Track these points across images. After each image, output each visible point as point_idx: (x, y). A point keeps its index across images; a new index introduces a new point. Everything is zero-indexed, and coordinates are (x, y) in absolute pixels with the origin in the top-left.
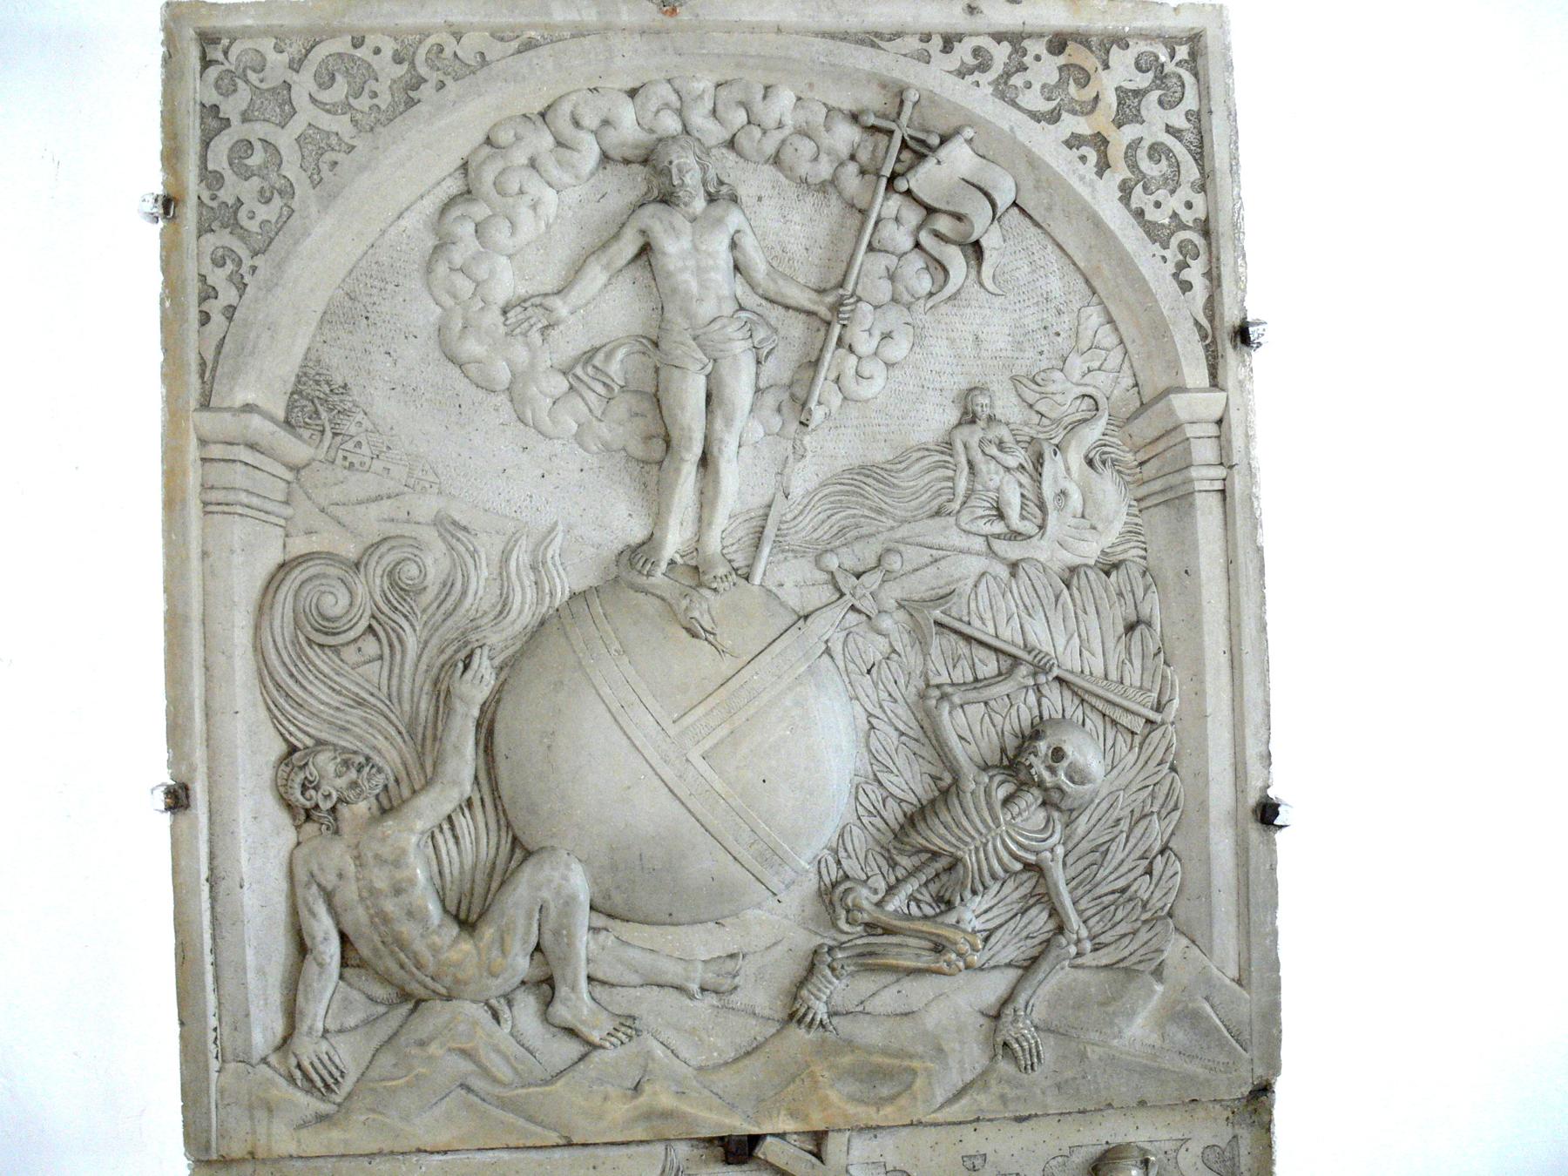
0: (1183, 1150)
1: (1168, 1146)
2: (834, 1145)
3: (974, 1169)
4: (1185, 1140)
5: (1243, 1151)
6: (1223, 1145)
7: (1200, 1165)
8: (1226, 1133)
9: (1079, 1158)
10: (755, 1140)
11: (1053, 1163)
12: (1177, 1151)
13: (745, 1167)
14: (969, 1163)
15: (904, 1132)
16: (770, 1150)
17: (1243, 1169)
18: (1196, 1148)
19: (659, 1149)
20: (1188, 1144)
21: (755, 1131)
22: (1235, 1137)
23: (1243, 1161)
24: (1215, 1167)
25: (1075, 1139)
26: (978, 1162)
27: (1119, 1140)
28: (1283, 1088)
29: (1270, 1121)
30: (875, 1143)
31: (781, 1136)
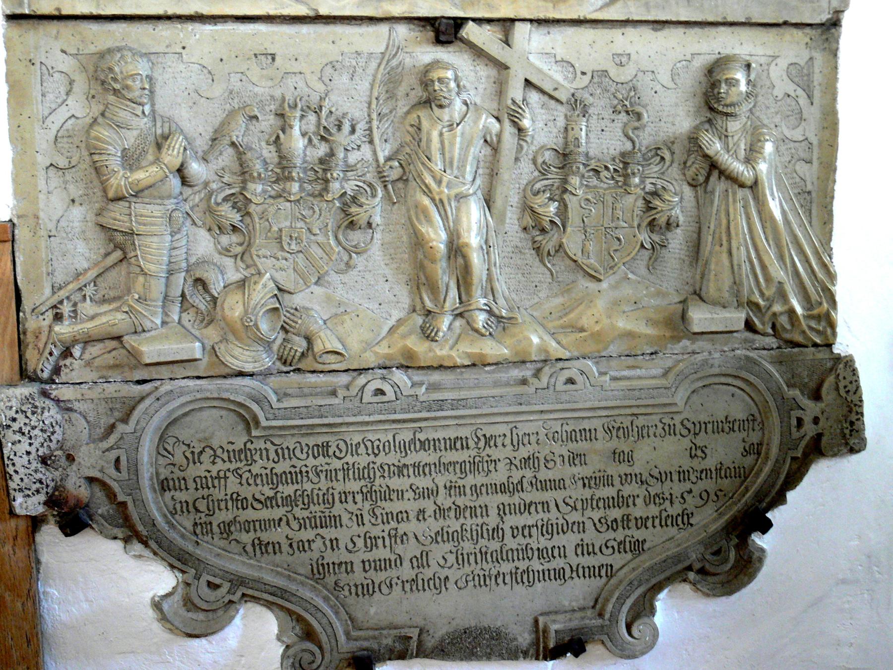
0: (773, 64)
1: (763, 60)
2: (521, 31)
3: (621, 65)
4: (775, 57)
5: (817, 70)
6: (802, 63)
7: (785, 77)
8: (806, 55)
9: (699, 63)
10: (459, 23)
11: (678, 65)
12: (769, 65)
13: (451, 48)
14: (617, 60)
15: (571, 31)
16: (470, 31)
17: (816, 83)
18: (783, 63)
19: (384, 28)
20: (778, 60)
21: (461, 14)
22: (811, 58)
23: (815, 78)
24: (796, 80)
25: (696, 48)
26: (624, 60)
27: (727, 51)
28: (846, 20)
29: (837, 49)
30: (548, 38)
31: (479, 21)
